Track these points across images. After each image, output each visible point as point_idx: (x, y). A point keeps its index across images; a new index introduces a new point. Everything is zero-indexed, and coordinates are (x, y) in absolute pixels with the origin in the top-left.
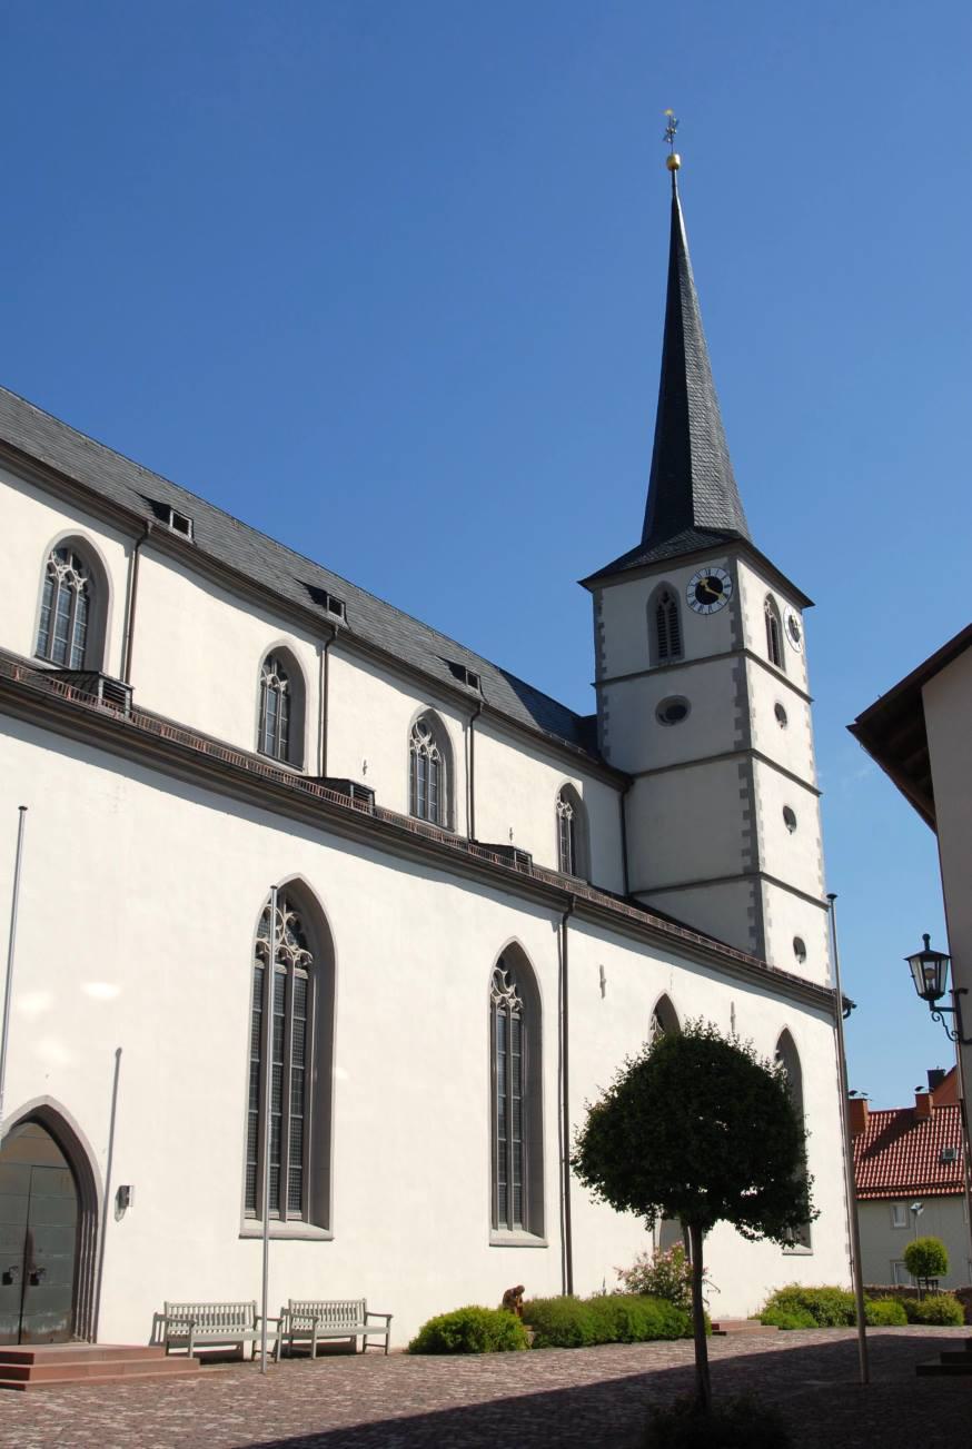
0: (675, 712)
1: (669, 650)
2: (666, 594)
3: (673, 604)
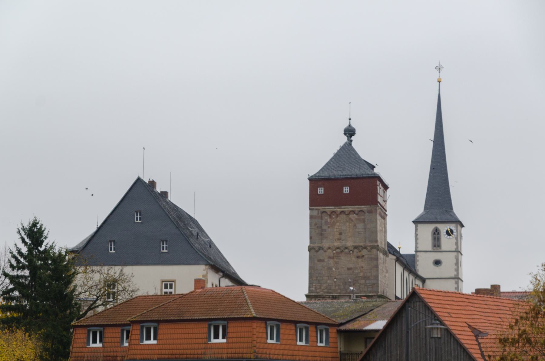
0: (437, 263)
1: (437, 246)
2: (436, 229)
3: (438, 233)
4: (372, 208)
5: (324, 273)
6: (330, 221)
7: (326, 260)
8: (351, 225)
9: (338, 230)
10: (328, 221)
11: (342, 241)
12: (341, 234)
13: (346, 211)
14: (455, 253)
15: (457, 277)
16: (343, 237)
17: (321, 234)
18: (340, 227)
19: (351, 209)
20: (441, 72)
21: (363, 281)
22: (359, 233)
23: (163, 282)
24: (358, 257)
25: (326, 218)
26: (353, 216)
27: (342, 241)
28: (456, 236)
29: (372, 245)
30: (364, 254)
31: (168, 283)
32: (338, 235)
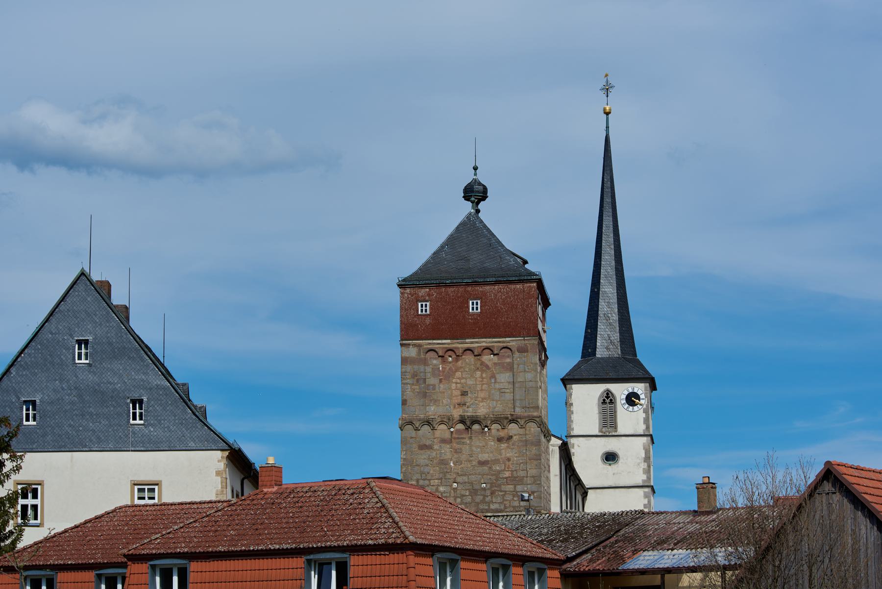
0: (610, 457)
3: (611, 400)
4: (526, 342)
5: (431, 472)
6: (442, 368)
7: (436, 447)
8: (484, 375)
9: (458, 385)
10: (439, 368)
11: (467, 409)
12: (464, 394)
13: (474, 347)
14: (645, 440)
15: (649, 484)
16: (468, 399)
17: (424, 395)
18: (463, 381)
19: (484, 344)
20: (610, 94)
21: (510, 488)
22: (501, 391)
23: (135, 484)
24: (500, 440)
25: (435, 362)
26: (488, 358)
27: (467, 409)
28: (645, 406)
29: (529, 416)
30: (511, 434)
31: (146, 487)
32: (460, 397)
